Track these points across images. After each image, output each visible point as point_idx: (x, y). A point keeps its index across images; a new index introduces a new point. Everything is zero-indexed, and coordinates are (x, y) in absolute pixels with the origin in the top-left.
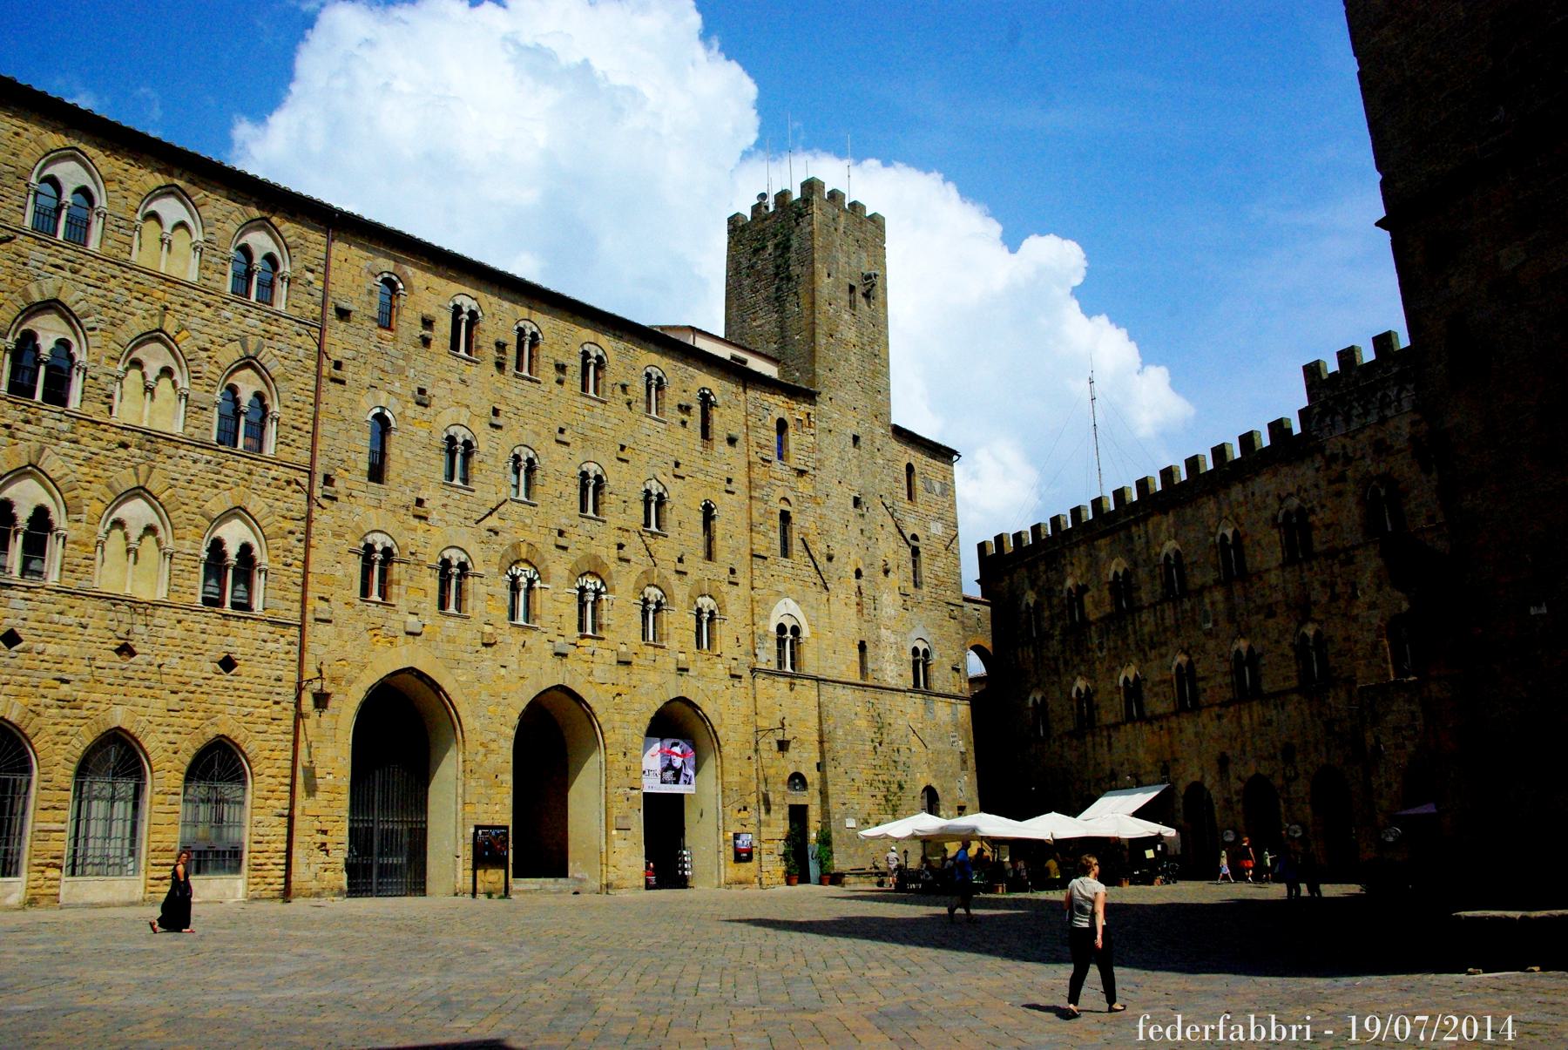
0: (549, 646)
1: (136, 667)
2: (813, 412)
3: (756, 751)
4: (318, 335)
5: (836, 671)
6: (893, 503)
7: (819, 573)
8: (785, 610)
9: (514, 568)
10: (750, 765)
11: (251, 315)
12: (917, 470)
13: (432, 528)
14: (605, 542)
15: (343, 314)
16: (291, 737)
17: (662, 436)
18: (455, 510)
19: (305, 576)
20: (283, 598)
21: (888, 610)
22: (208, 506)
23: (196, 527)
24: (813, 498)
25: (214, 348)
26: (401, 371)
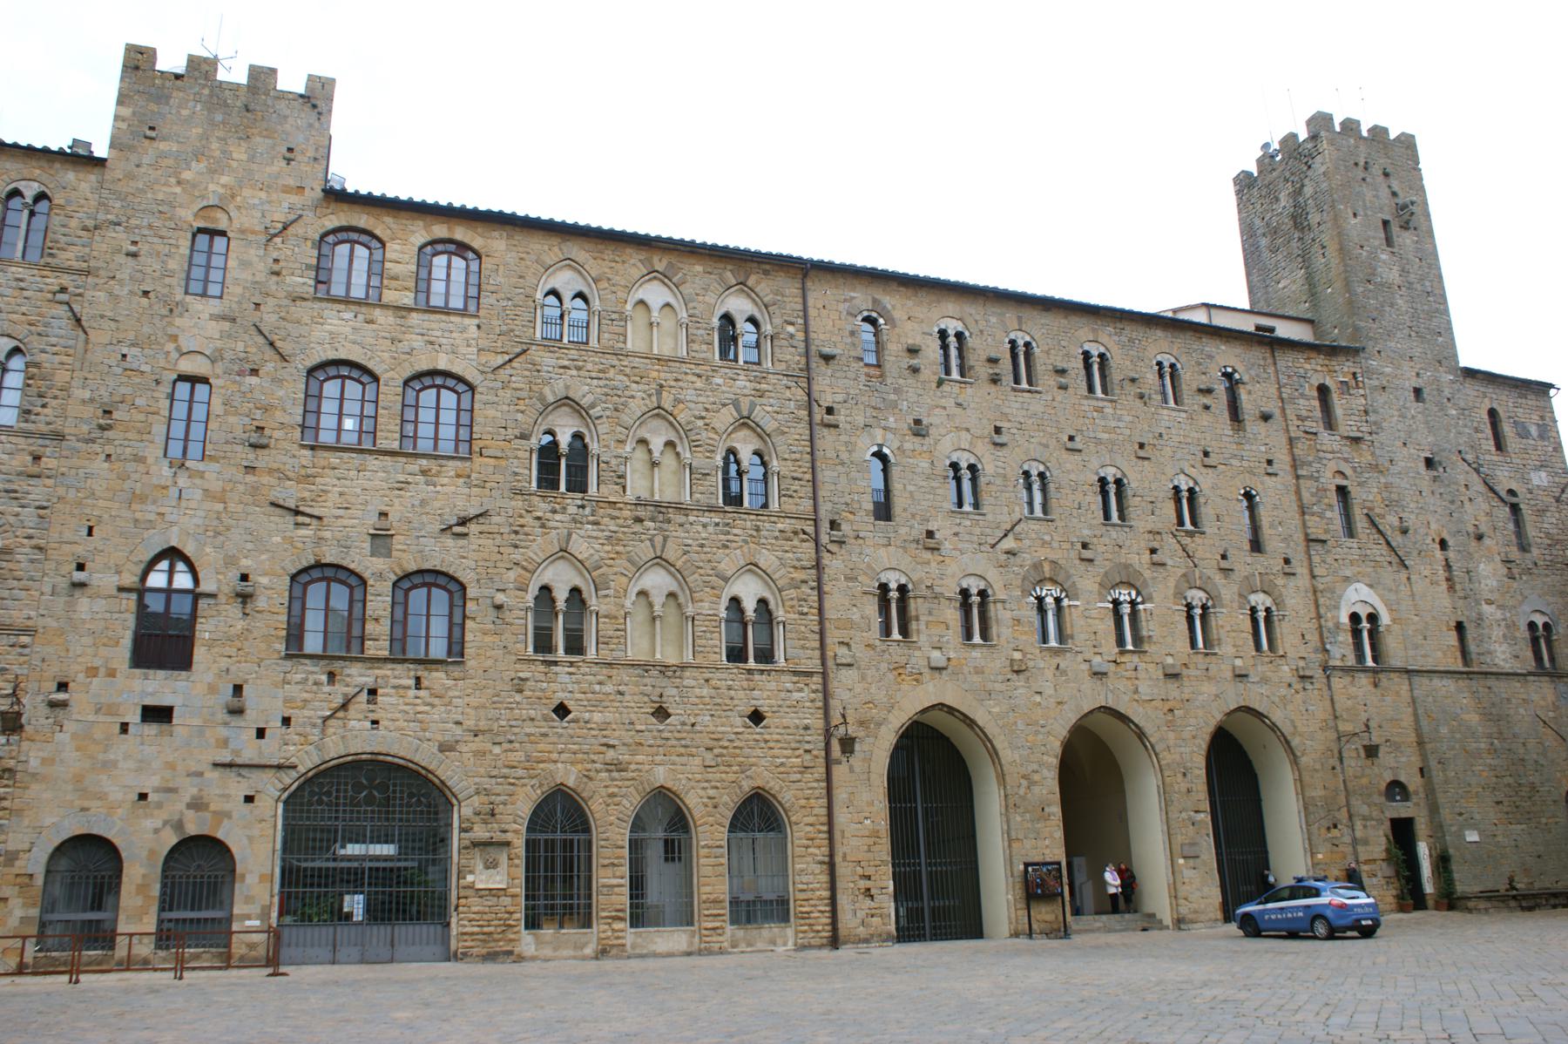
0: (1085, 666)
1: (672, 728)
2: (1358, 370)
3: (1341, 759)
4: (806, 385)
5: (1430, 660)
6: (1477, 457)
7: (1393, 549)
8: (1358, 596)
9: (1038, 589)
10: (1335, 775)
11: (741, 377)
13: (947, 560)
14: (1135, 548)
15: (827, 358)
16: (824, 784)
17: (1183, 426)
18: (967, 537)
19: (821, 622)
20: (803, 647)
21: (1489, 582)
22: (722, 566)
23: (713, 588)
24: (1375, 467)
25: (709, 415)
26: (894, 405)
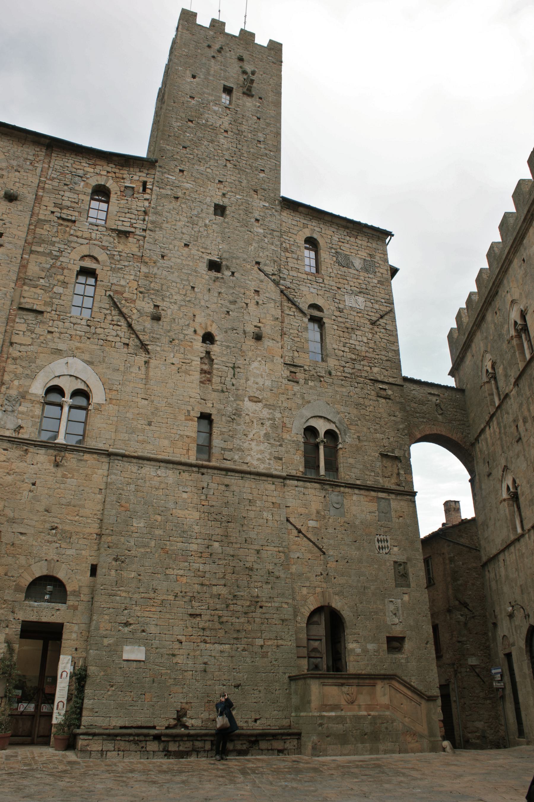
5: (149, 447)
12: (322, 242)
